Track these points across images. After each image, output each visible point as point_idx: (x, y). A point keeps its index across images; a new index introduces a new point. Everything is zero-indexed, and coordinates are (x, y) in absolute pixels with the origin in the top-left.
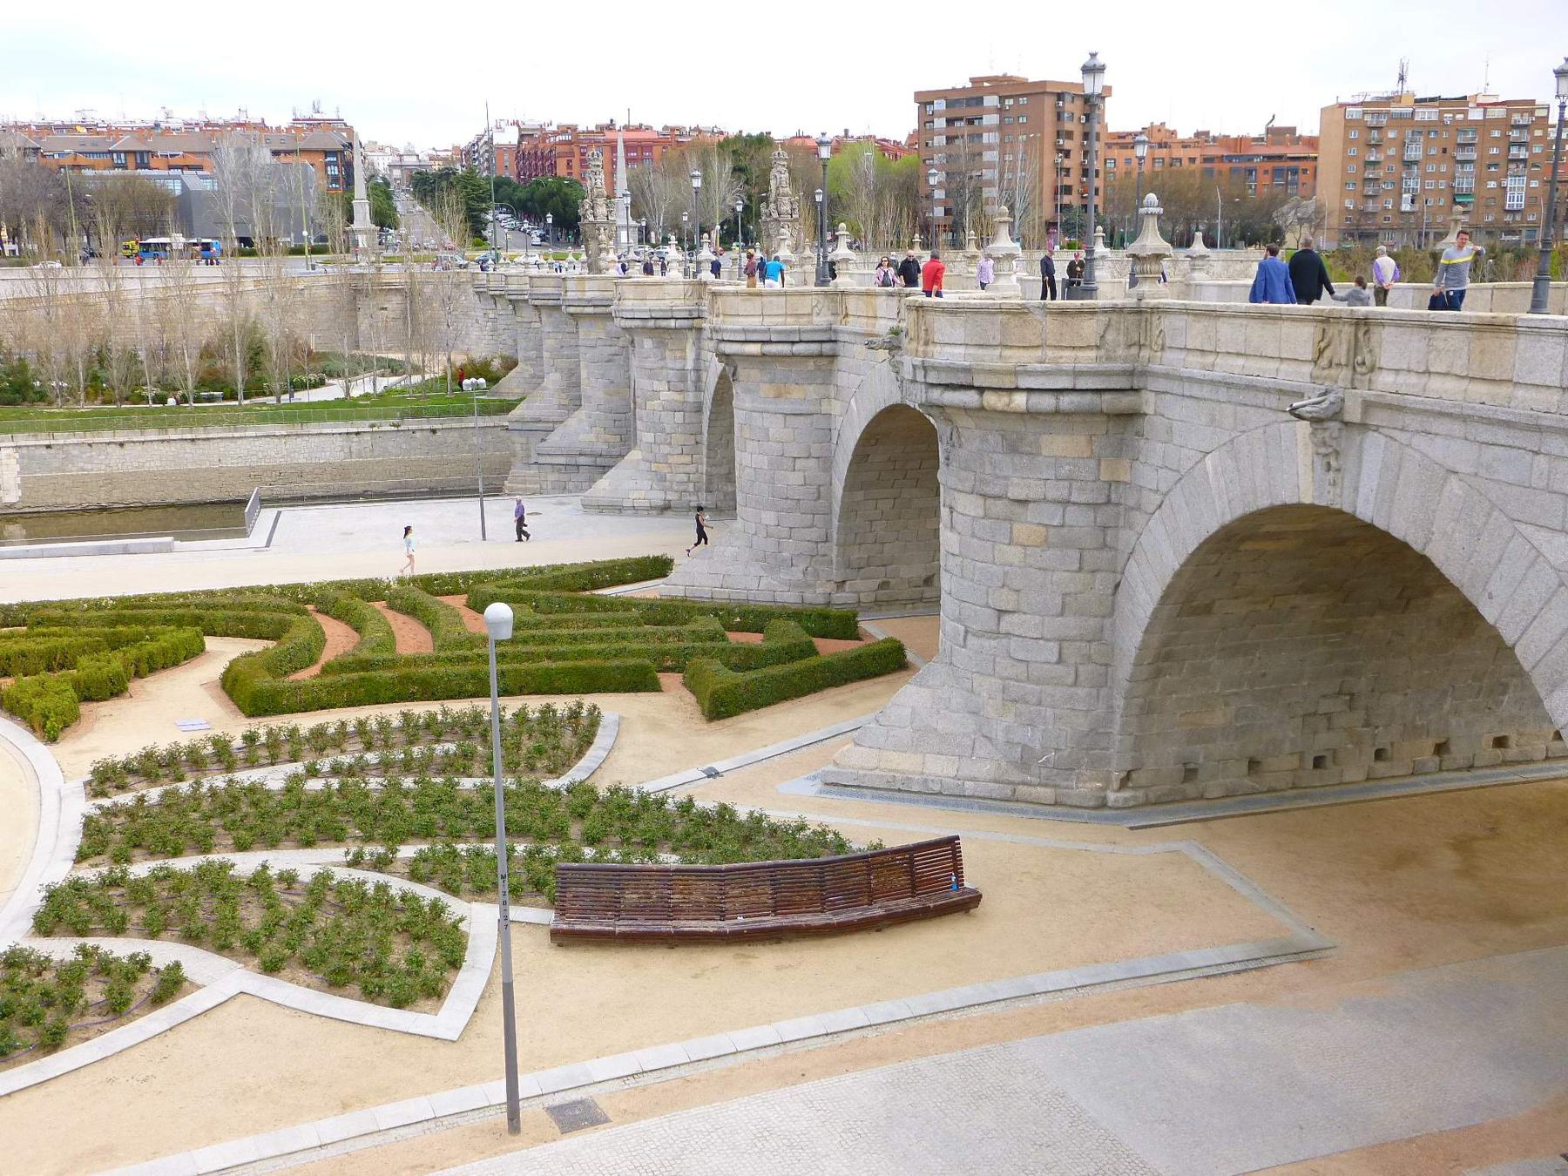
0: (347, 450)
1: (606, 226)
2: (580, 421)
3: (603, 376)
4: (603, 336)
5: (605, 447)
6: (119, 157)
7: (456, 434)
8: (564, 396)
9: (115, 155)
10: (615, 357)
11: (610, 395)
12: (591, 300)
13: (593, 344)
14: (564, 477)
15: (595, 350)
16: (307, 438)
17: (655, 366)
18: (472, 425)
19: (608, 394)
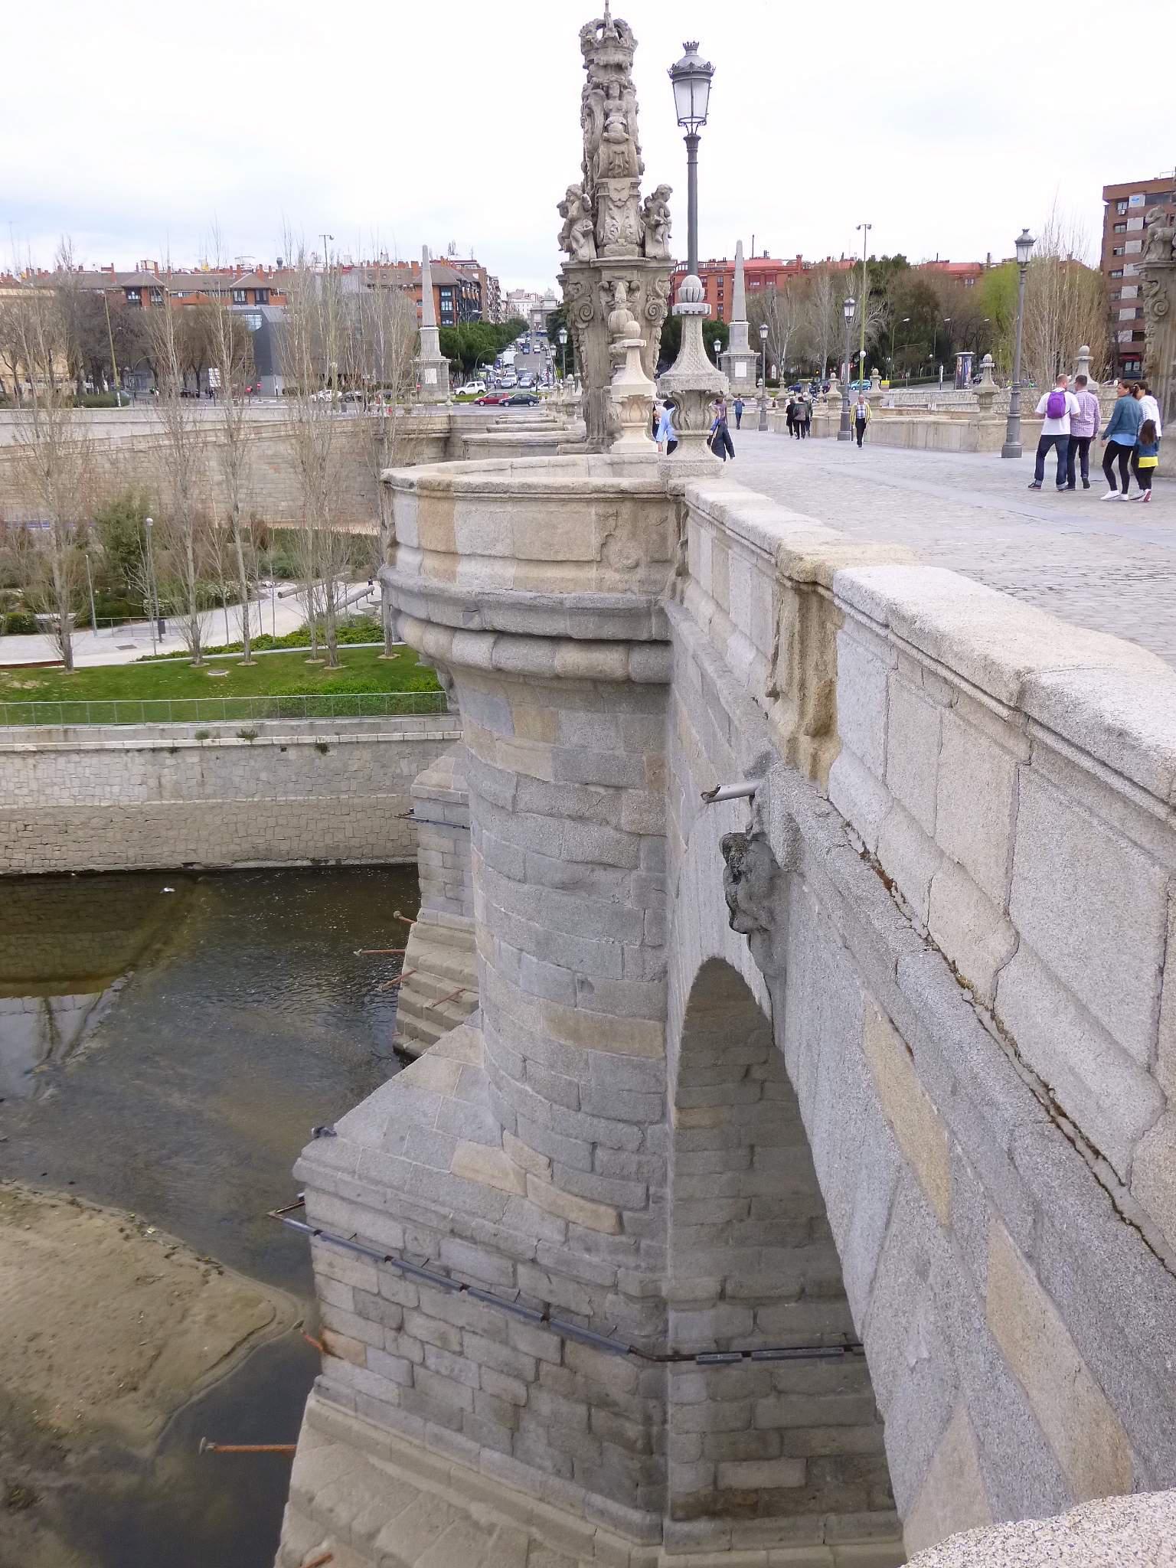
0: (152, 782)
1: (636, 277)
3: (544, 947)
5: (551, 1232)
6: (239, 295)
7: (367, 754)
9: (236, 293)
10: (602, 876)
11: (575, 1034)
12: (474, 606)
16: (75, 758)
18: (397, 736)
19: (557, 1023)
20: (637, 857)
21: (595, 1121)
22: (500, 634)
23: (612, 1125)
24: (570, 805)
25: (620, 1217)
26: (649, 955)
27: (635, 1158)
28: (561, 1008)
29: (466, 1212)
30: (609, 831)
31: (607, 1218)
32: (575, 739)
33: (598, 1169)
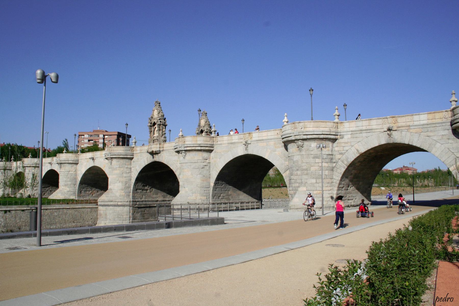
8: (123, 191)
15: (197, 164)
17: (317, 153)
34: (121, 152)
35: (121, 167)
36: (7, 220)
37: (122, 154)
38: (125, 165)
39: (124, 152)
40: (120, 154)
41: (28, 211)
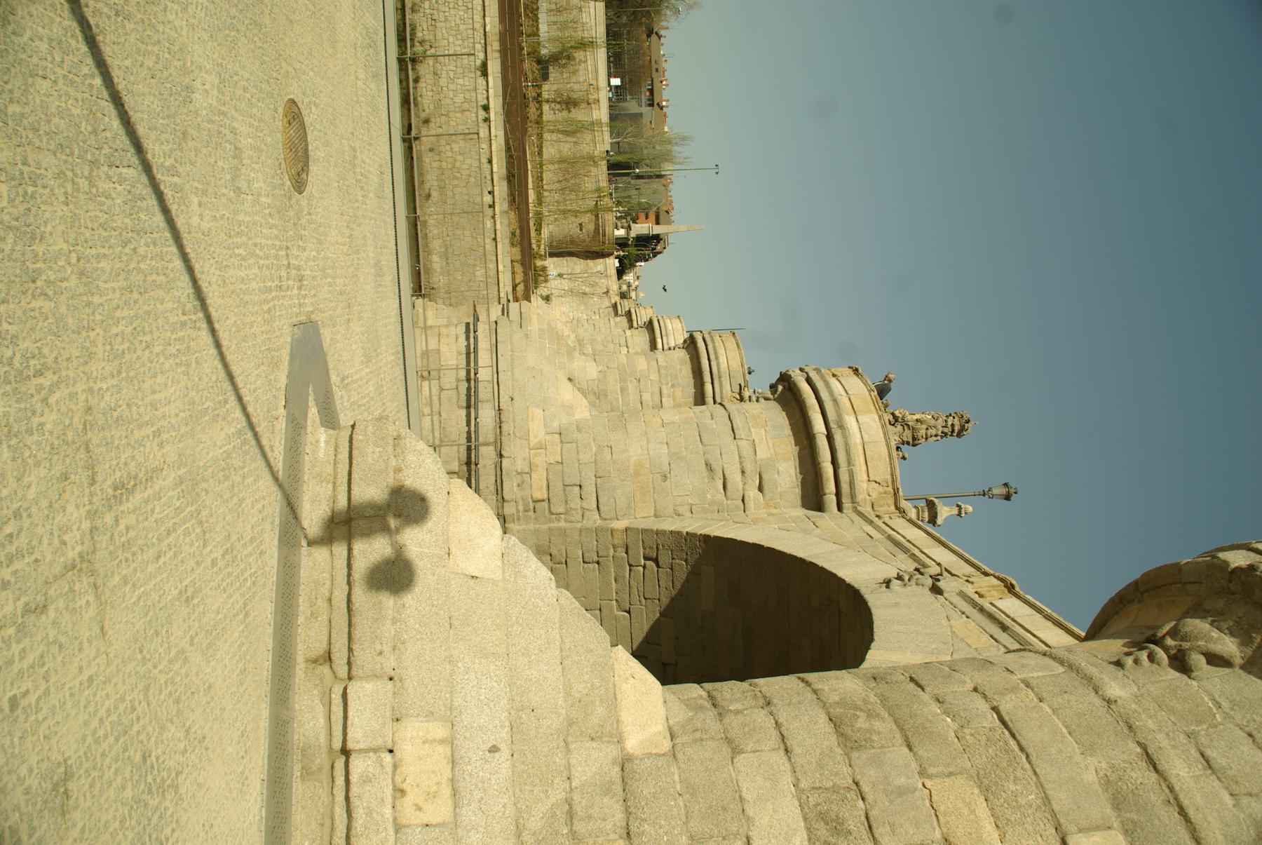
2: (569, 409)
4: (762, 454)
5: (521, 465)
12: (842, 426)
13: (741, 433)
14: (449, 380)
20: (732, 500)
21: (594, 486)
22: (830, 437)
23: (595, 495)
24: (749, 467)
25: (543, 500)
26: (687, 508)
27: (578, 507)
28: (648, 466)
29: (514, 417)
30: (741, 485)
31: (541, 494)
32: (781, 468)
33: (567, 488)
34: (723, 360)
35: (663, 372)
36: (459, 115)
37: (714, 364)
38: (673, 386)
39: (722, 370)
40: (712, 357)
41: (489, 178)
